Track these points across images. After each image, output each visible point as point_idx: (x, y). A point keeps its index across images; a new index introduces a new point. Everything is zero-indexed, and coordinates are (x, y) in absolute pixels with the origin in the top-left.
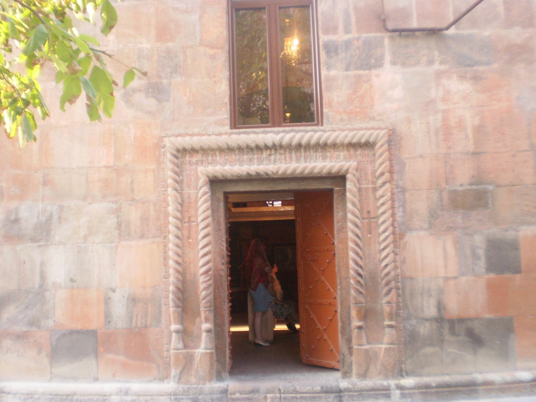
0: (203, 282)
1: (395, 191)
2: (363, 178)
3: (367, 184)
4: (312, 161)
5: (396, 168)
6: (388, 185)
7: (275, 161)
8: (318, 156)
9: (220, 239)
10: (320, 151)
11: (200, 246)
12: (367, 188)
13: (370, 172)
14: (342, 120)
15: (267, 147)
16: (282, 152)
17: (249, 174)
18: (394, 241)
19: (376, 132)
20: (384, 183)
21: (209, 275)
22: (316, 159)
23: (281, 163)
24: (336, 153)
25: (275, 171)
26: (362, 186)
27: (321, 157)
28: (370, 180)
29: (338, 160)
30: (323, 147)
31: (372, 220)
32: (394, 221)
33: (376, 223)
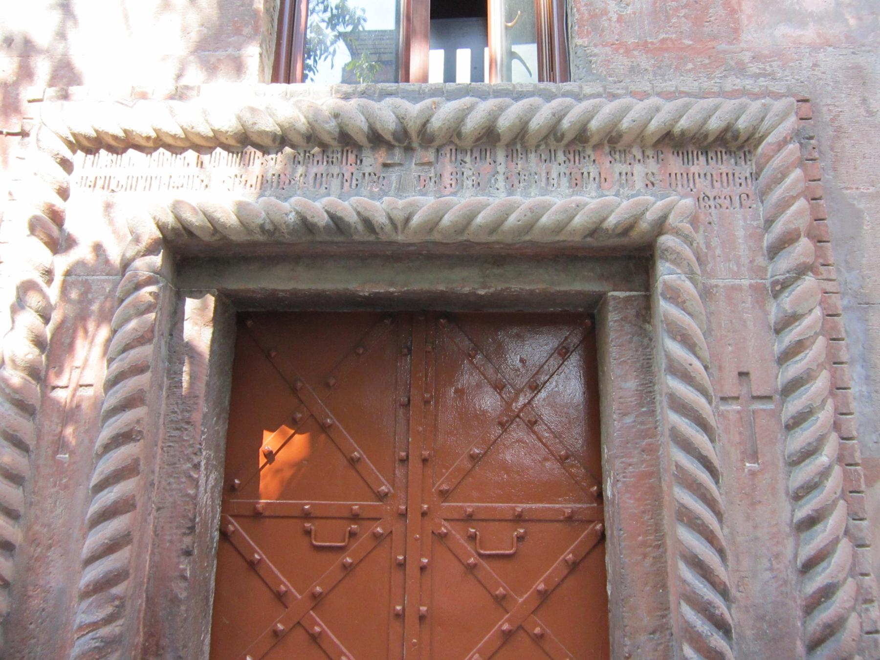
0: (81, 628)
1: (839, 303)
2: (718, 252)
3: (736, 275)
4: (533, 191)
5: (832, 225)
6: (809, 281)
7: (401, 189)
8: (554, 175)
9: (189, 460)
10: (561, 157)
11: (95, 479)
12: (739, 288)
13: (740, 233)
14: (634, 70)
15: (376, 139)
16: (430, 155)
17: (306, 225)
18: (851, 491)
19: (755, 106)
20: (801, 271)
21: (115, 598)
22: (548, 183)
23: (424, 194)
24: (619, 167)
25: (399, 216)
26: (713, 282)
27: (564, 181)
28: (745, 261)
29: (626, 191)
30: (575, 143)
31: (758, 406)
32: (842, 412)
33: (775, 415)
